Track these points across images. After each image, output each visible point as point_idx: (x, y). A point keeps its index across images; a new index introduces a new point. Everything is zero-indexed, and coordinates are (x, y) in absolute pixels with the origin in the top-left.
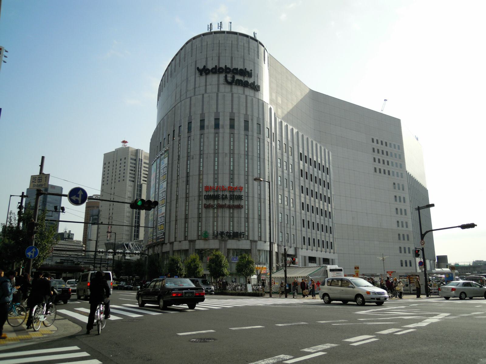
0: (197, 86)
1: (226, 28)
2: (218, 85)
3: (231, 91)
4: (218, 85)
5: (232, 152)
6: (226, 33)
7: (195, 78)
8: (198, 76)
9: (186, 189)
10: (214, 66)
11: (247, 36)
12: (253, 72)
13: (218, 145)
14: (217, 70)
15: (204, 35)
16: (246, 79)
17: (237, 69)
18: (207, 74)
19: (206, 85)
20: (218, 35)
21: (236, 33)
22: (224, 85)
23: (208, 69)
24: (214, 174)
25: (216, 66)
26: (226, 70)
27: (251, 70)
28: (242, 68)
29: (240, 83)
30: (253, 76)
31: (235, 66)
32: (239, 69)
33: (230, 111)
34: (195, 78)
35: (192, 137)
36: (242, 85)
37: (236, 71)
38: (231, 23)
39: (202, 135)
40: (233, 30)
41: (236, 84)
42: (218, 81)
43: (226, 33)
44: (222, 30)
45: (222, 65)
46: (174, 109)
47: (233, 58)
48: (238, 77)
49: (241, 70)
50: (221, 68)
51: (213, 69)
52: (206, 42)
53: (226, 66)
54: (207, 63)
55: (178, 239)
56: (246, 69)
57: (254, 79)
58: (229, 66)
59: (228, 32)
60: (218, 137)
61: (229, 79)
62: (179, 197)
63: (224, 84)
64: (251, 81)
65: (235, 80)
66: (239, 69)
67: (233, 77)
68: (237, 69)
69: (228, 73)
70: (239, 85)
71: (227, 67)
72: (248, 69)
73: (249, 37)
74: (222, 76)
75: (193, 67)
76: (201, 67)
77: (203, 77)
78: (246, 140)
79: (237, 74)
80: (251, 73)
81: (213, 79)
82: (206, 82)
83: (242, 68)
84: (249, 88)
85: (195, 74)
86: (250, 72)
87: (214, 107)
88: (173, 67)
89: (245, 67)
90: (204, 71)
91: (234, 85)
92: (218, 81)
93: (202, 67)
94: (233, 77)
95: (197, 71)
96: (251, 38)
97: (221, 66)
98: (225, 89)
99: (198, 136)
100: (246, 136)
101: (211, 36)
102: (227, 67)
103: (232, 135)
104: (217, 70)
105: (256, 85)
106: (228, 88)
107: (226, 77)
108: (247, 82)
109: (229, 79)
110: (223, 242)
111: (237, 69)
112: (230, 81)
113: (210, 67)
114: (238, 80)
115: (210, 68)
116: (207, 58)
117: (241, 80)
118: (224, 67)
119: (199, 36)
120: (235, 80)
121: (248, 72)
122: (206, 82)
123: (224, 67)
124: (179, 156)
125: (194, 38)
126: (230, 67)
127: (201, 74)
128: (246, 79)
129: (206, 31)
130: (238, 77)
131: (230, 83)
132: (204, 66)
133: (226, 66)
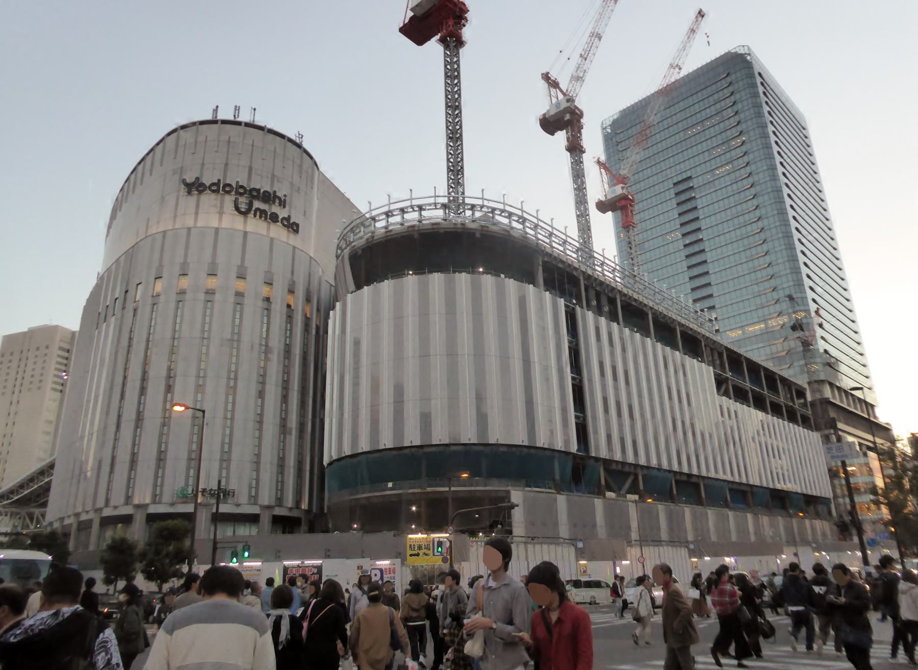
1: (244, 117)
6: (243, 124)
7: (178, 199)
8: (183, 196)
9: (139, 403)
10: (216, 181)
11: (282, 136)
13: (210, 323)
15: (202, 123)
16: (275, 209)
17: (259, 190)
20: (228, 126)
21: (261, 128)
23: (203, 185)
24: (198, 377)
25: (219, 180)
26: (240, 190)
31: (255, 184)
32: (262, 191)
33: (239, 263)
34: (178, 199)
35: (161, 306)
37: (254, 194)
38: (255, 109)
39: (181, 303)
43: (243, 124)
46: (131, 249)
47: (253, 170)
49: (265, 192)
52: (204, 138)
53: (238, 182)
54: (202, 172)
55: (112, 503)
57: (290, 211)
59: (247, 125)
60: (212, 309)
61: (243, 207)
64: (282, 213)
66: (262, 191)
67: (250, 205)
68: (259, 190)
69: (241, 194)
73: (286, 138)
74: (229, 200)
75: (177, 177)
76: (190, 179)
77: (192, 200)
78: (265, 318)
79: (257, 198)
82: (197, 206)
83: (269, 190)
85: (179, 191)
86: (283, 198)
87: (208, 253)
88: (139, 175)
89: (275, 189)
90: (195, 187)
93: (193, 180)
94: (250, 205)
95: (183, 186)
97: (228, 182)
100: (266, 311)
104: (217, 188)
105: (291, 222)
109: (243, 207)
110: (204, 510)
111: (258, 191)
112: (243, 210)
116: (203, 165)
119: (194, 124)
121: (280, 199)
122: (197, 206)
124: (130, 339)
125: (183, 127)
127: (189, 193)
128: (275, 209)
129: (209, 116)
130: (257, 204)
131: (245, 214)
132: (197, 179)
133: (238, 182)
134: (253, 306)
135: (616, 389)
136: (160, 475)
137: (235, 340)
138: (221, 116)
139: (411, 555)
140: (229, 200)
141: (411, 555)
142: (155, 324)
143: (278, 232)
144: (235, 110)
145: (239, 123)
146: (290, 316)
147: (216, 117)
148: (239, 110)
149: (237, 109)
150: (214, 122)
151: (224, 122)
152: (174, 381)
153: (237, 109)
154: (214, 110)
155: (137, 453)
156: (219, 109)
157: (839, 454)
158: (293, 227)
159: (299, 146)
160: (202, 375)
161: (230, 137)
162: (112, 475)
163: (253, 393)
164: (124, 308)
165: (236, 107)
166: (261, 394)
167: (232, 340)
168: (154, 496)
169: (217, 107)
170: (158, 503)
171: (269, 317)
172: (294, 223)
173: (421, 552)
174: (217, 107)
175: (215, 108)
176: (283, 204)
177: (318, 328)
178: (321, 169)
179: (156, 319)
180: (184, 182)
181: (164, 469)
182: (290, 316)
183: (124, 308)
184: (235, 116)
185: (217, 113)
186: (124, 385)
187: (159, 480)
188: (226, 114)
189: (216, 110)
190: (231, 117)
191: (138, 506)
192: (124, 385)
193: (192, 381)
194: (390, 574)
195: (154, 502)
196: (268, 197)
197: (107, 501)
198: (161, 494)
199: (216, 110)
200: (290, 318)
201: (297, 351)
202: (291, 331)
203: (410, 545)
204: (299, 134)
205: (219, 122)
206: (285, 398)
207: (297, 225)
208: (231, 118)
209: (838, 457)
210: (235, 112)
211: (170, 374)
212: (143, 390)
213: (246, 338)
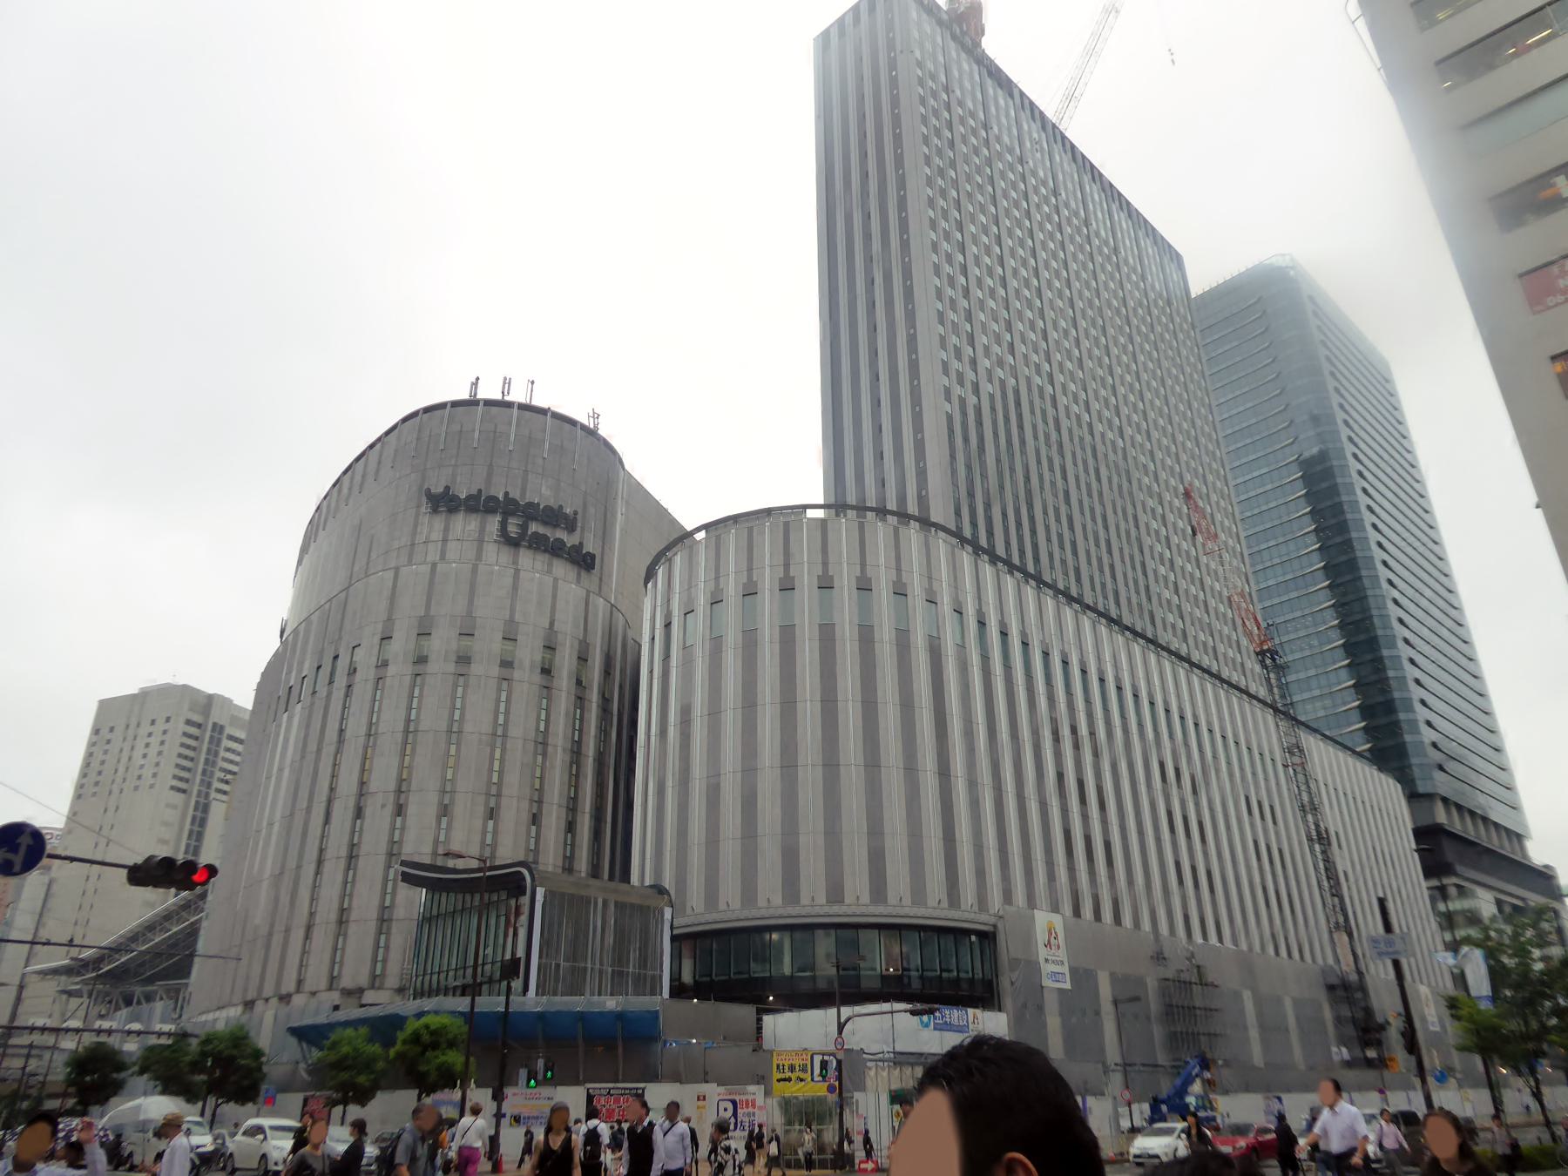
0: (420, 538)
1: (518, 395)
2: (481, 541)
3: (515, 562)
4: (481, 541)
5: (500, 732)
10: (474, 492)
12: (579, 517)
14: (479, 504)
15: (455, 404)
17: (538, 504)
18: (452, 510)
19: (445, 540)
20: (494, 410)
22: (497, 545)
23: (455, 498)
25: (480, 491)
26: (508, 508)
27: (576, 513)
29: (539, 544)
30: (579, 529)
32: (541, 507)
33: (507, 617)
36: (545, 551)
37: (530, 512)
38: (533, 382)
39: (419, 678)
40: (537, 402)
41: (530, 547)
42: (482, 530)
44: (507, 398)
48: (534, 527)
50: (494, 499)
51: (469, 497)
52: (459, 428)
53: (506, 494)
55: (308, 987)
56: (561, 507)
57: (582, 537)
58: (515, 494)
59: (523, 407)
62: (318, 920)
63: (495, 541)
64: (570, 540)
65: (529, 533)
66: (541, 507)
67: (524, 527)
68: (538, 504)
69: (513, 514)
70: (537, 549)
71: (511, 496)
73: (579, 427)
74: (494, 522)
77: (438, 522)
79: (534, 519)
81: (465, 525)
82: (446, 530)
84: (566, 559)
85: (418, 507)
88: (358, 478)
90: (444, 503)
91: (525, 546)
92: (482, 530)
94: (524, 527)
95: (424, 499)
96: (584, 428)
97: (493, 493)
98: (496, 557)
99: (407, 680)
102: (511, 496)
103: (505, 684)
104: (479, 504)
106: (506, 555)
107: (503, 524)
109: (513, 530)
114: (535, 533)
115: (463, 496)
117: (546, 538)
120: (529, 533)
121: (566, 516)
122: (446, 530)
123: (501, 497)
124: (341, 731)
125: (427, 410)
127: (435, 511)
129: (466, 396)
130: (534, 527)
131: (512, 543)
132: (447, 488)
133: (506, 494)
134: (526, 678)
135: (1085, 817)
136: (382, 944)
137: (499, 735)
138: (482, 394)
139: (779, 1081)
140: (494, 522)
141: (779, 1081)
143: (561, 569)
144: (504, 383)
145: (509, 405)
146: (580, 698)
147: (475, 395)
148: (509, 383)
149: (507, 382)
150: (472, 403)
151: (489, 403)
152: (407, 798)
153: (507, 382)
154: (473, 384)
155: (350, 908)
157: (1390, 950)
158: (584, 562)
159: (591, 433)
160: (448, 789)
161: (496, 426)
162: (308, 941)
163: (525, 817)
164: (331, 682)
165: (505, 379)
166: (535, 819)
167: (494, 734)
168: (374, 977)
169: (478, 379)
170: (379, 988)
171: (549, 699)
173: (793, 1076)
174: (478, 379)
175: (474, 381)
176: (571, 526)
178: (627, 467)
181: (388, 934)
182: (580, 698)
183: (331, 682)
184: (503, 393)
185: (476, 388)
186: (330, 802)
187: (381, 951)
188: (491, 391)
189: (475, 384)
190: (497, 396)
191: (347, 993)
192: (330, 802)
193: (433, 798)
194: (747, 1107)
195: (372, 987)
196: (554, 517)
197: (300, 982)
198: (383, 975)
199: (475, 384)
200: (580, 700)
201: (590, 750)
202: (582, 720)
203: (778, 1066)
205: (481, 404)
206: (571, 827)
207: (593, 557)
208: (498, 397)
209: (1388, 953)
211: (400, 786)
212: (359, 813)
213: (515, 731)
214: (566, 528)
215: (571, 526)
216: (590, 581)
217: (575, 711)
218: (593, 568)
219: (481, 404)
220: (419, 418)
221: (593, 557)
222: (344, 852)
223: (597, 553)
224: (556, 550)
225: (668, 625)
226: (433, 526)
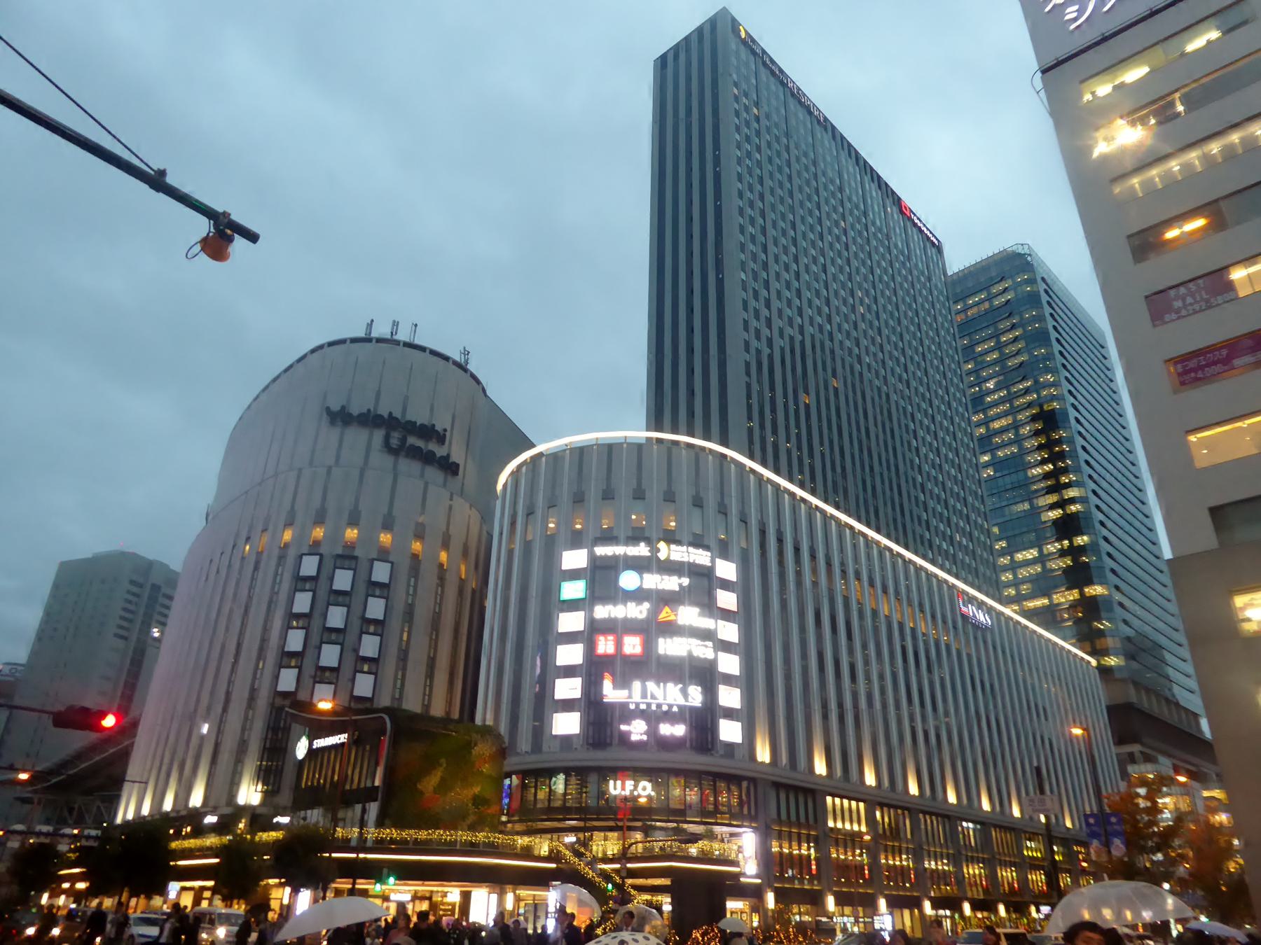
1: (402, 336)
10: (365, 411)
12: (448, 434)
14: (370, 420)
15: (354, 340)
16: (433, 446)
21: (423, 349)
23: (350, 415)
25: (369, 410)
26: (389, 423)
27: (445, 430)
28: (426, 423)
32: (418, 424)
38: (416, 325)
40: (417, 342)
41: (407, 456)
44: (396, 337)
45: (384, 411)
48: (412, 440)
49: (422, 426)
50: (381, 416)
51: (361, 415)
53: (390, 414)
56: (434, 425)
58: (397, 414)
64: (440, 451)
66: (418, 424)
67: (403, 440)
68: (416, 423)
72: (439, 428)
74: (379, 435)
76: (335, 407)
77: (335, 433)
80: (445, 435)
81: (357, 437)
86: (442, 433)
89: (434, 422)
90: (341, 418)
93: (339, 408)
94: (403, 440)
98: (380, 460)
101: (367, 345)
105: (451, 461)
106: (389, 460)
108: (433, 453)
109: (394, 442)
112: (395, 446)
113: (355, 410)
117: (419, 448)
118: (386, 415)
126: (400, 418)
128: (433, 446)
129: (362, 334)
130: (412, 440)
132: (343, 408)
133: (390, 414)
138: (375, 334)
140: (379, 435)
142: (281, 581)
143: (434, 474)
144: (394, 325)
145: (397, 343)
147: (370, 333)
149: (395, 324)
150: (367, 340)
151: (379, 340)
153: (395, 324)
156: (374, 323)
159: (462, 367)
165: (394, 321)
169: (372, 321)
172: (455, 463)
174: (372, 321)
176: (441, 439)
177: (474, 591)
179: (282, 574)
180: (328, 410)
184: (392, 333)
188: (381, 330)
189: (370, 325)
196: (428, 432)
199: (370, 325)
200: (442, 579)
204: (465, 350)
205: (374, 341)
207: (458, 465)
210: (393, 329)
214: (438, 442)
215: (441, 439)
216: (455, 483)
217: (437, 589)
218: (457, 474)
219: (374, 341)
220: (324, 350)
221: (458, 465)
222: (246, 694)
223: (461, 463)
224: (427, 458)
225: (513, 523)
226: (332, 435)
